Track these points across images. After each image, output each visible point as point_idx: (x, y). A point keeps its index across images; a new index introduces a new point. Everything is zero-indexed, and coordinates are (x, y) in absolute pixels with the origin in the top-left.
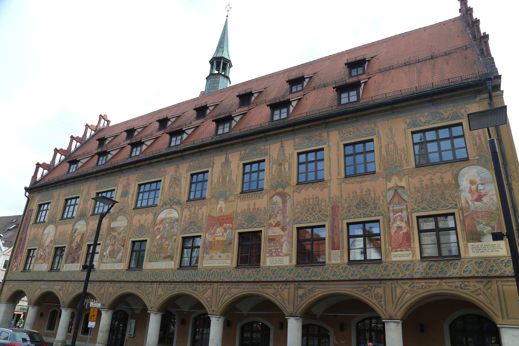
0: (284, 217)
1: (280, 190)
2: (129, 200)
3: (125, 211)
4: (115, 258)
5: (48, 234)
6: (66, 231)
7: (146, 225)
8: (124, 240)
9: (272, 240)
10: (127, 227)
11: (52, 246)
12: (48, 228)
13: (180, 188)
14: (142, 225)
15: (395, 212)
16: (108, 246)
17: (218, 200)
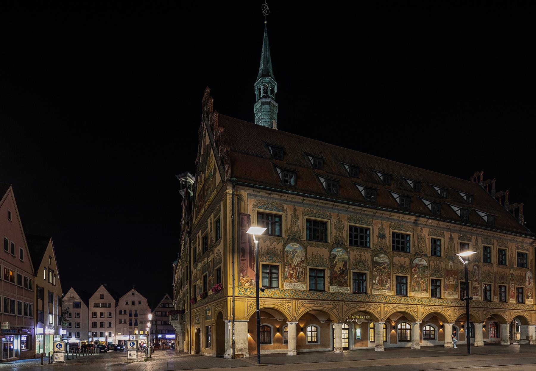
0: (479, 278)
1: (477, 263)
2: (388, 243)
3: (385, 251)
4: (385, 286)
5: (294, 253)
6: (321, 254)
7: (405, 265)
8: (390, 274)
9: (474, 288)
10: (390, 264)
11: (306, 267)
12: (289, 245)
13: (426, 245)
14: (402, 265)
15: (512, 284)
16: (376, 276)
17: (449, 260)
